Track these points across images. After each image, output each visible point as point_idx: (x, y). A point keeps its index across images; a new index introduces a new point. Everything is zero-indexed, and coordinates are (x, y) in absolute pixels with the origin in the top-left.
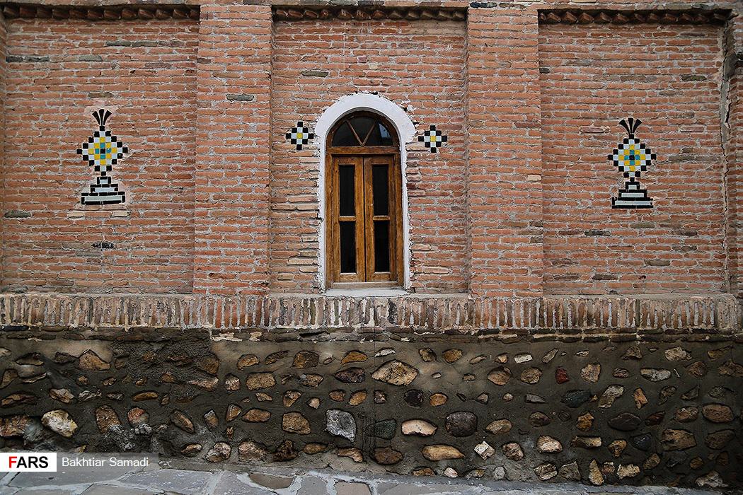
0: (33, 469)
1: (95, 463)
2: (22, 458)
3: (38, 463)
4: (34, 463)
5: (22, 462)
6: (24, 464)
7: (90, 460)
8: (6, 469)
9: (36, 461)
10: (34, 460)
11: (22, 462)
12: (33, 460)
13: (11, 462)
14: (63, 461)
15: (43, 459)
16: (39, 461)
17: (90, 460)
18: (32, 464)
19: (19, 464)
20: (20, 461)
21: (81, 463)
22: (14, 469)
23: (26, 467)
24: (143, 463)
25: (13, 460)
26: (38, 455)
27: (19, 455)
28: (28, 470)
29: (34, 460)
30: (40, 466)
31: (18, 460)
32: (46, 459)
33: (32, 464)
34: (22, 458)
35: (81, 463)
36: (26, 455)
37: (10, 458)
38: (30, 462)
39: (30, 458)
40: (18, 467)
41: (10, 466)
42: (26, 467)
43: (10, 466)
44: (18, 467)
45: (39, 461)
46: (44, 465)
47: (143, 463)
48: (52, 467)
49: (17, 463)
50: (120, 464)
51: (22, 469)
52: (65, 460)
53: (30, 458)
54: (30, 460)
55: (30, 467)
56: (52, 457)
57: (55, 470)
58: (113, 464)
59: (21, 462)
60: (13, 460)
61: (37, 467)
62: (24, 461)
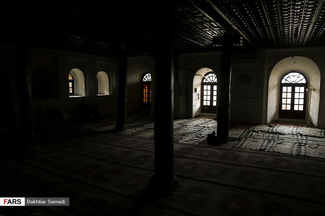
0: (14, 205)
1: (42, 202)
2: (10, 200)
3: (17, 202)
4: (15, 202)
5: (10, 202)
6: (11, 203)
7: (39, 201)
8: (3, 205)
9: (16, 201)
10: (15, 201)
11: (10, 202)
12: (14, 201)
13: (5, 202)
14: (28, 201)
15: (19, 200)
16: (17, 201)
17: (39, 201)
18: (14, 203)
19: (8, 203)
20: (9, 201)
21: (36, 202)
22: (6, 205)
23: (11, 204)
24: (62, 202)
25: (6, 201)
26: (17, 199)
27: (8, 198)
28: (12, 205)
29: (15, 201)
30: (18, 203)
31: (8, 201)
32: (20, 200)
33: (14, 203)
34: (10, 200)
35: (36, 202)
36: (11, 199)
37: (5, 200)
38: (13, 202)
39: (13, 200)
40: (8, 204)
41: (5, 204)
42: (11, 204)
43: (5, 204)
44: (8, 204)
45: (17, 201)
46: (19, 203)
47: (62, 202)
48: (23, 204)
49: (8, 202)
50: (60, 203)
51: (10, 205)
52: (29, 201)
53: (13, 200)
54: (13, 201)
55: (13, 204)
56: (23, 200)
57: (24, 205)
58: (50, 202)
59: (9, 202)
60: (6, 201)
61: (16, 204)
62: (10, 201)
